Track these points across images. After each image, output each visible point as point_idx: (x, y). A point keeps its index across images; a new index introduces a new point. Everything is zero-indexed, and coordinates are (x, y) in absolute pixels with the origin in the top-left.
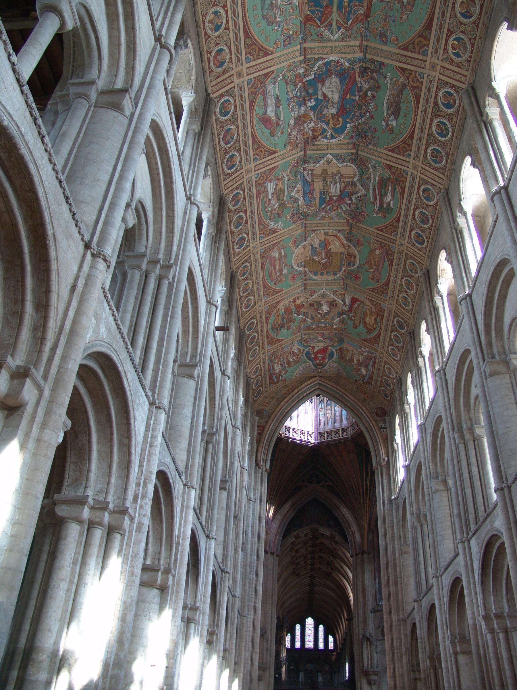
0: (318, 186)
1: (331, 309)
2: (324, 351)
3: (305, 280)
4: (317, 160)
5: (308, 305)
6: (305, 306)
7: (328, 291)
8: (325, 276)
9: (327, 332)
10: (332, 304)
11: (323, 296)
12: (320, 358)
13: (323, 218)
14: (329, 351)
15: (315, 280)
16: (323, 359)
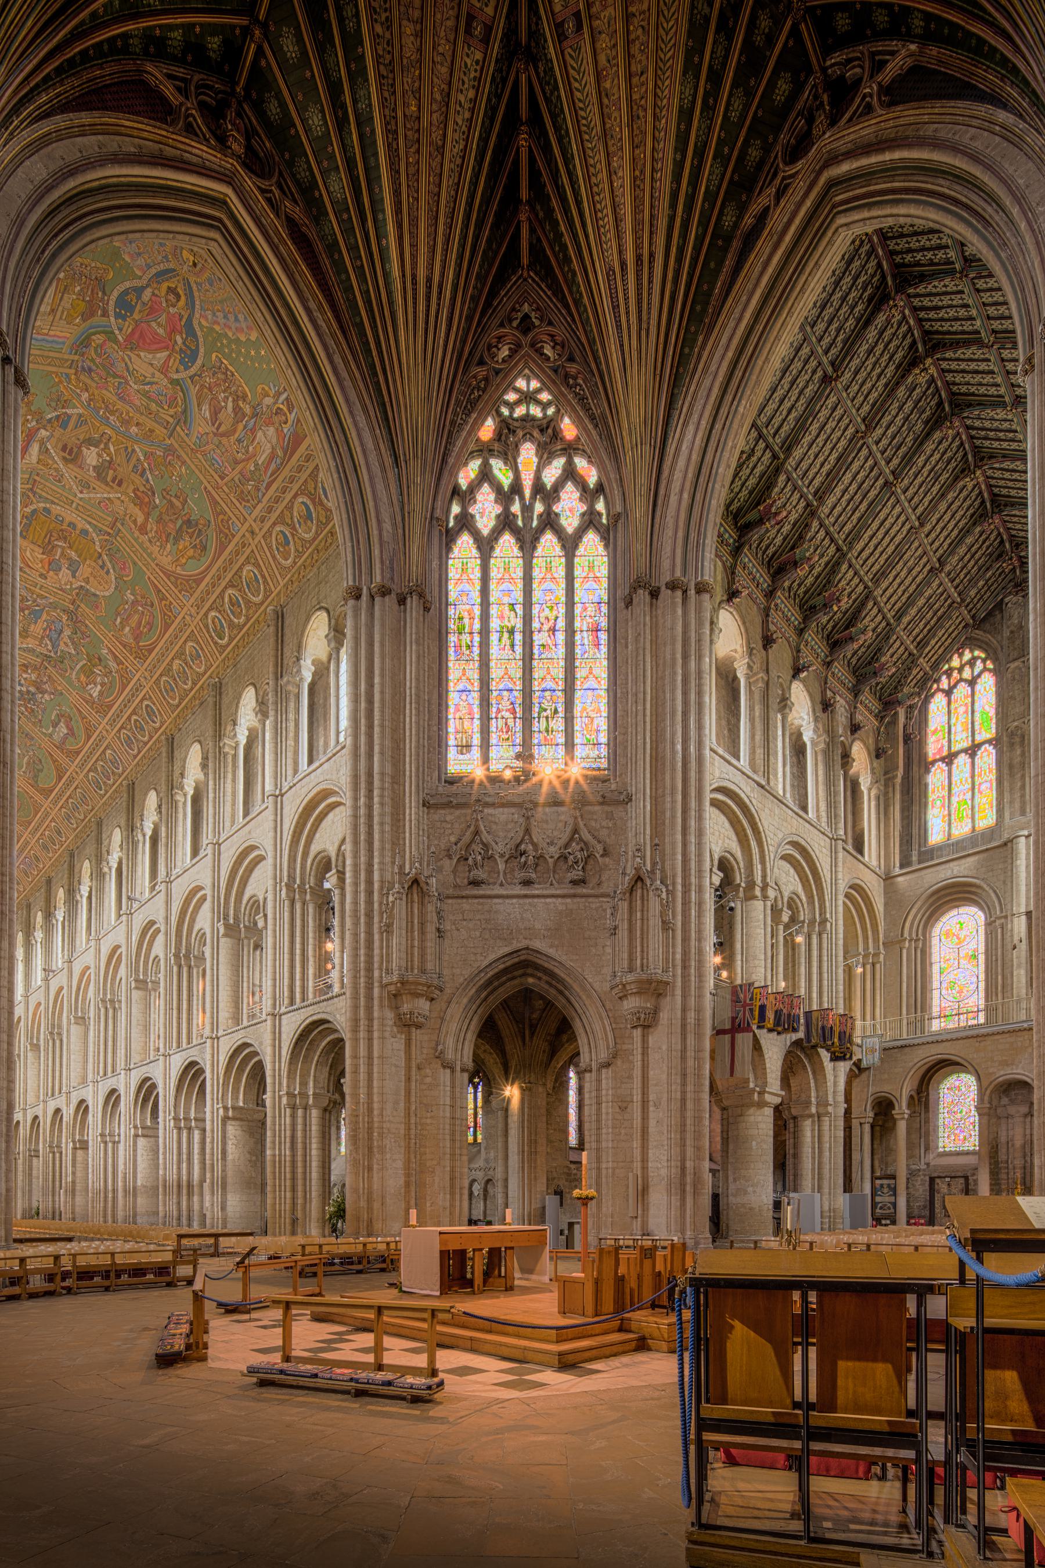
0: (37, 629)
1: (79, 448)
2: (137, 341)
3: (109, 534)
4: (32, 651)
5: (124, 485)
6: (132, 487)
7: (71, 489)
8: (68, 519)
9: (110, 396)
10: (72, 455)
11: (85, 486)
12: (163, 319)
13: (43, 597)
14: (128, 327)
15: (90, 523)
16: (153, 310)
